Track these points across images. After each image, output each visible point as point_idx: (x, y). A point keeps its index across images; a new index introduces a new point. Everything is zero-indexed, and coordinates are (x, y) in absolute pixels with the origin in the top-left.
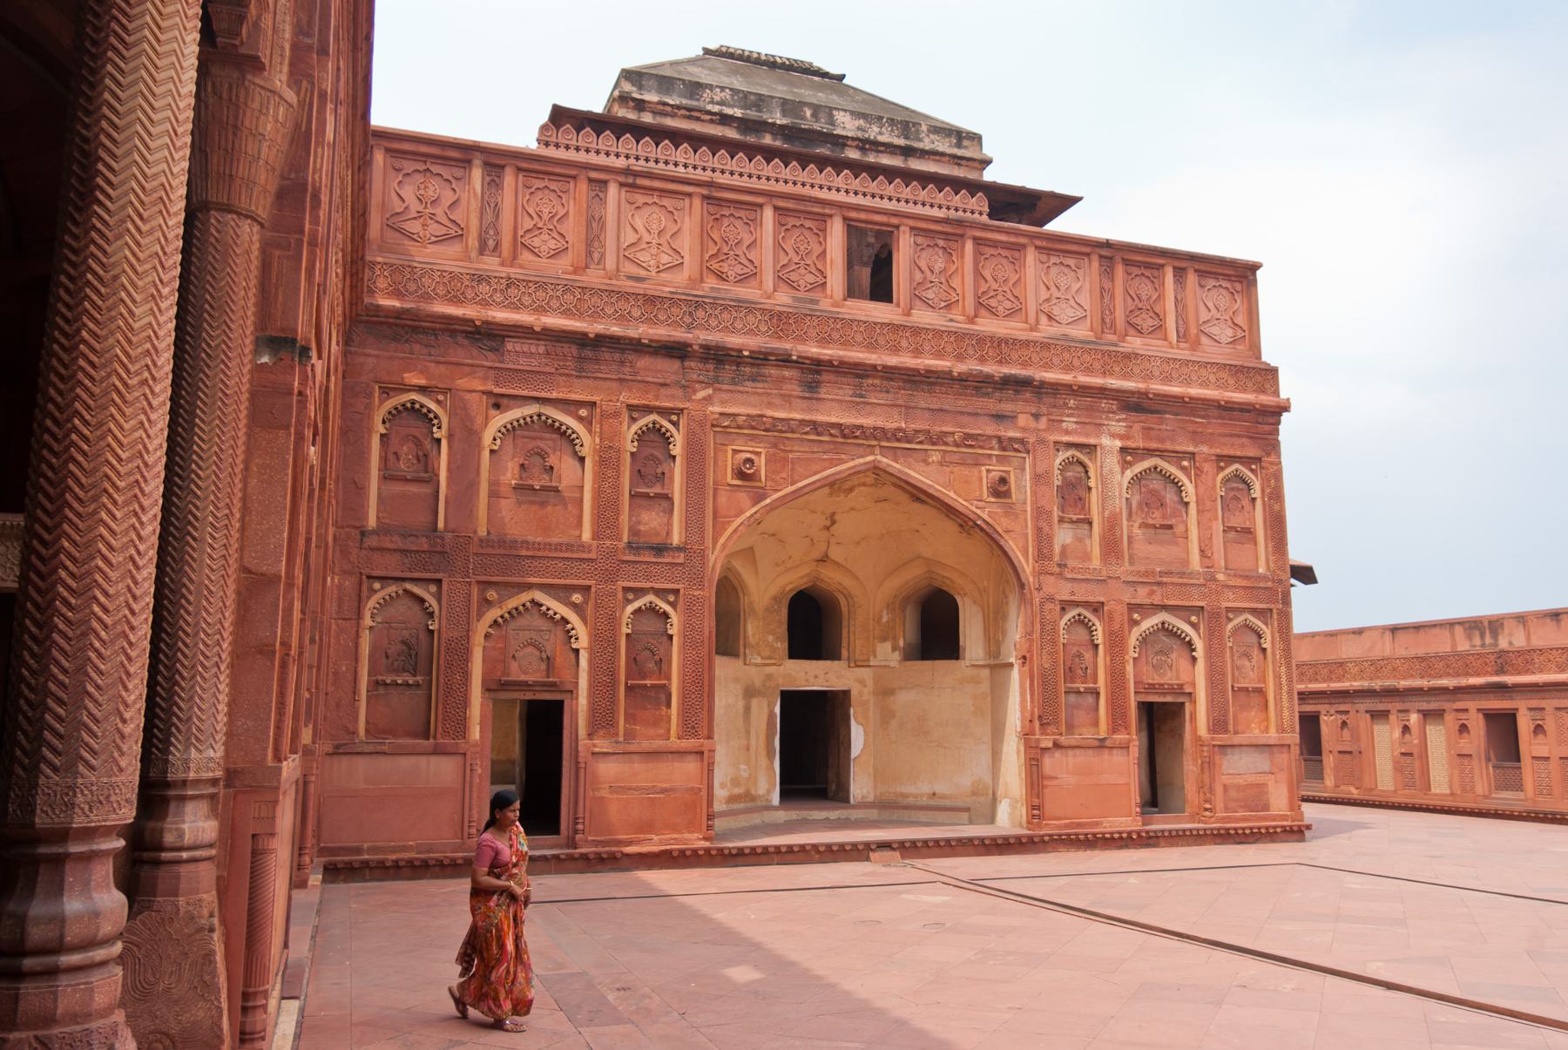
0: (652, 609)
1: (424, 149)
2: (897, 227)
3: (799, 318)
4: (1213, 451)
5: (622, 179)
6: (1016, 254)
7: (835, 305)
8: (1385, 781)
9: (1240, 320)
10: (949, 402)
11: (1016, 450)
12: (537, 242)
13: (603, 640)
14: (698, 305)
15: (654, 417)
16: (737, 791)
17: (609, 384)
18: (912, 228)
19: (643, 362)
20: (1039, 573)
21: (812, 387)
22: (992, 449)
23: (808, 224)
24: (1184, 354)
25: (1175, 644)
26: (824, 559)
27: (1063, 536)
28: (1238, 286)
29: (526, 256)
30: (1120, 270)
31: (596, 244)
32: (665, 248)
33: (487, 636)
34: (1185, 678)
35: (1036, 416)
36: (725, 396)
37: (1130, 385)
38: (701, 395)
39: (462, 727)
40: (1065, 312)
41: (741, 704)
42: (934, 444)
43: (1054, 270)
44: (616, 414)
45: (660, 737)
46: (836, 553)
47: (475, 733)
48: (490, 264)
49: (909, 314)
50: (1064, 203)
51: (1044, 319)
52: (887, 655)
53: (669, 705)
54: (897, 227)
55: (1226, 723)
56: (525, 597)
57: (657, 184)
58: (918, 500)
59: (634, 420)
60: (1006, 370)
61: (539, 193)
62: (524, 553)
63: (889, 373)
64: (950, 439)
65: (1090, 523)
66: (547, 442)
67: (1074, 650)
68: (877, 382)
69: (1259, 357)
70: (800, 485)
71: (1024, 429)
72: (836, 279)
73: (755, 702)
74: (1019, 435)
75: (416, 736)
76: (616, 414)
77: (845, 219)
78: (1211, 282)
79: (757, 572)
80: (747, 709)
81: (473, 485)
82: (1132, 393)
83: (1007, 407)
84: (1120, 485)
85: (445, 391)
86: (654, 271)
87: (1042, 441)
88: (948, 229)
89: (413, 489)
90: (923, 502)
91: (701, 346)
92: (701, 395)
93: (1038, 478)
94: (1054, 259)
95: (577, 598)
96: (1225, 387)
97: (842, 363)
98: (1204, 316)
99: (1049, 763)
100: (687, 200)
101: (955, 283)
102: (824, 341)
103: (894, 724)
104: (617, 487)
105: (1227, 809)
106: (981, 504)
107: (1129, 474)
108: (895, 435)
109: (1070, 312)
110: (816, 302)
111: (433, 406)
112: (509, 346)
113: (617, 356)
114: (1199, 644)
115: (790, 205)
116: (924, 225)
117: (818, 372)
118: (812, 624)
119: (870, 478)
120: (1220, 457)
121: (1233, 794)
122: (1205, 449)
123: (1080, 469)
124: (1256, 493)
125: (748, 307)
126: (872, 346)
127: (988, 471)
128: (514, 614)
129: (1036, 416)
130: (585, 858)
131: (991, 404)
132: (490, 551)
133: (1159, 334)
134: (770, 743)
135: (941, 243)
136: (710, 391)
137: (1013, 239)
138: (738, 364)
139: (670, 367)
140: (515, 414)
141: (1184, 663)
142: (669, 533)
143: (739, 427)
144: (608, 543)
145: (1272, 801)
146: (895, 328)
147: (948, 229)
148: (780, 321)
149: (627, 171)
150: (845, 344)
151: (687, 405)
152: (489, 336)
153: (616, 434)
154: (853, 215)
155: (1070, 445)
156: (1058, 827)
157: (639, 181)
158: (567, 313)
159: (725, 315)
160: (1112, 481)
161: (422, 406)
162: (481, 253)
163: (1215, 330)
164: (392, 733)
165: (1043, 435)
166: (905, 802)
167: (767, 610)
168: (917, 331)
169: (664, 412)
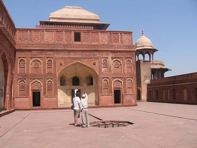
0: (50, 81)
7: (73, 43)
8: (185, 98)
10: (87, 53)
13: (44, 84)
16: (65, 102)
26: (76, 73)
27: (103, 69)
30: (112, 34)
33: (31, 85)
34: (120, 86)
36: (58, 55)
37: (112, 50)
39: (29, 95)
46: (77, 72)
47: (30, 95)
50: (108, 25)
52: (85, 85)
56: (35, 80)
60: (95, 49)
66: (38, 62)
72: (73, 39)
73: (68, 91)
75: (24, 96)
81: (29, 68)
83: (95, 54)
85: (25, 58)
87: (100, 58)
89: (23, 68)
93: (100, 62)
95: (41, 80)
98: (124, 39)
102: (70, 48)
107: (113, 61)
114: (122, 82)
120: (126, 58)
121: (127, 101)
128: (34, 82)
130: (43, 109)
131: (93, 53)
139: (51, 53)
140: (33, 59)
146: (79, 45)
149: (46, 29)
152: (30, 51)
153: (46, 61)
155: (104, 58)
157: (48, 30)
160: (111, 62)
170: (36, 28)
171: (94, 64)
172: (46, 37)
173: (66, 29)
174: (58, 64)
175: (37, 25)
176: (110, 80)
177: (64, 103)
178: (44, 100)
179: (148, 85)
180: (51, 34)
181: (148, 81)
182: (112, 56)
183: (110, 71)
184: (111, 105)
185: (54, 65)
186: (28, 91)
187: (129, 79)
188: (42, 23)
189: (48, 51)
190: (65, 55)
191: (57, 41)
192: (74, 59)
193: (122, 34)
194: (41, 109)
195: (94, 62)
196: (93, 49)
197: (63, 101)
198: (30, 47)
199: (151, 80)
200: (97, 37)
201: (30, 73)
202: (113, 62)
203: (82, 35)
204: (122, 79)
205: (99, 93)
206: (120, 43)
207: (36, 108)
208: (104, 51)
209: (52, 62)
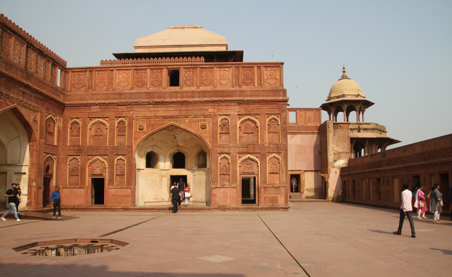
0: (121, 159)
1: (78, 70)
6: (211, 70)
7: (165, 89)
12: (100, 85)
13: (111, 165)
15: (122, 119)
20: (213, 146)
23: (158, 71)
24: (260, 88)
25: (253, 162)
26: (178, 146)
28: (277, 69)
30: (241, 69)
38: (131, 113)
41: (158, 179)
43: (222, 72)
44: (113, 119)
49: (182, 88)
51: (219, 84)
55: (266, 182)
57: (124, 68)
64: (191, 117)
66: (102, 126)
69: (283, 86)
75: (77, 185)
76: (113, 119)
77: (167, 68)
80: (161, 180)
87: (215, 115)
88: (193, 67)
89: (76, 137)
92: (131, 113)
94: (222, 69)
95: (106, 157)
98: (266, 77)
99: (214, 191)
108: (177, 117)
111: (79, 121)
114: (259, 162)
116: (186, 67)
118: (179, 161)
119: (174, 127)
121: (267, 199)
123: (226, 121)
124: (279, 123)
126: (171, 97)
128: (94, 161)
133: (252, 84)
135: (191, 70)
137: (210, 66)
141: (255, 167)
145: (279, 201)
146: (176, 92)
147: (193, 67)
148: (149, 94)
150: (164, 98)
153: (115, 124)
154: (169, 67)
163: (269, 81)
164: (73, 184)
168: (182, 92)
170: (101, 66)
171: (203, 127)
172: (118, 80)
173: (152, 64)
174: (135, 129)
175: (102, 61)
178: (110, 191)
179: (342, 170)
180: (126, 75)
181: (342, 162)
182: (238, 112)
184: (234, 205)
188: (119, 56)
193: (262, 68)
194: (104, 209)
195: (203, 123)
198: (88, 100)
199: (350, 161)
200: (210, 75)
201: (88, 145)
202: (242, 123)
203: (183, 75)
204: (258, 156)
206: (256, 85)
209: (126, 125)
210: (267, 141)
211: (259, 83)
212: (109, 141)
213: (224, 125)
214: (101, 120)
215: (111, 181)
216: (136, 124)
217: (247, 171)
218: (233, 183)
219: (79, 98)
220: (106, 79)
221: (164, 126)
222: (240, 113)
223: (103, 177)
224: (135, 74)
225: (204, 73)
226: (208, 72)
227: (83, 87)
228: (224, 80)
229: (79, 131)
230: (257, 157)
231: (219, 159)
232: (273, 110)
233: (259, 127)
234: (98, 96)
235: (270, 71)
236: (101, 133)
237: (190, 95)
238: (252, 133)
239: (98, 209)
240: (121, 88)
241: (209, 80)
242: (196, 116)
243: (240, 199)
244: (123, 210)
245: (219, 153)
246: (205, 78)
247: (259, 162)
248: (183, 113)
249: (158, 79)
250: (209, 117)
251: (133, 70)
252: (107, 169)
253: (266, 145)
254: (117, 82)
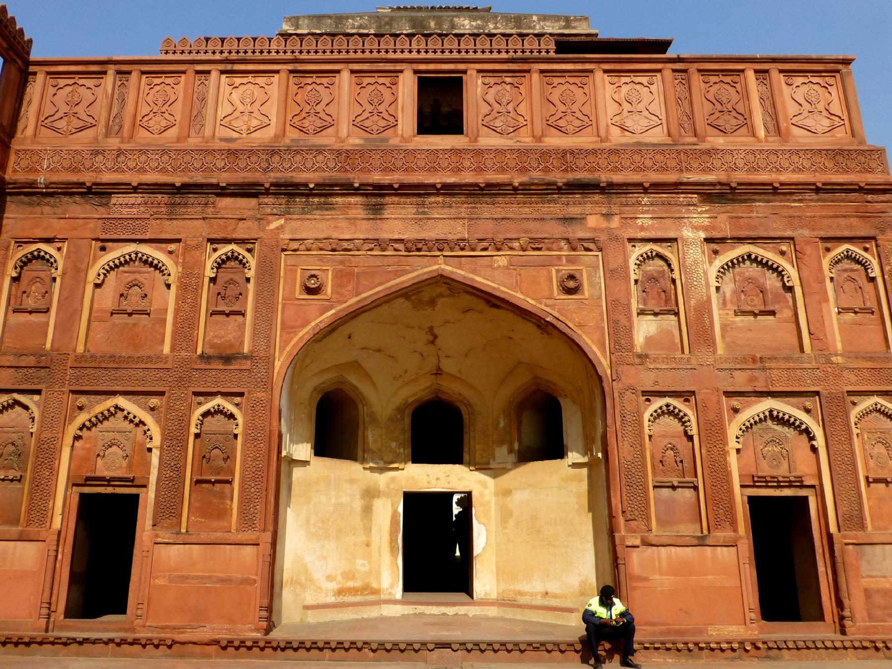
2: (465, 72)
3: (361, 152)
4: (816, 233)
5: (222, 67)
9: (836, 108)
11: (587, 249)
13: (174, 439)
14: (273, 152)
17: (195, 222)
18: (479, 71)
19: (225, 202)
21: (376, 210)
22: (561, 249)
29: (143, 133)
30: (697, 80)
31: (199, 118)
32: (256, 114)
35: (608, 216)
36: (295, 224)
38: (274, 225)
40: (636, 123)
42: (499, 250)
44: (198, 247)
45: (221, 529)
48: (114, 143)
49: (476, 141)
51: (615, 131)
53: (232, 500)
54: (465, 72)
55: (862, 518)
58: (495, 306)
59: (215, 250)
60: (571, 176)
61: (158, 88)
62: (111, 365)
63: (449, 190)
64: (516, 245)
65: (677, 314)
67: (665, 442)
68: (440, 199)
70: (363, 295)
71: (595, 230)
74: (588, 235)
76: (198, 247)
78: (799, 80)
79: (374, 385)
82: (713, 184)
83: (574, 211)
84: (705, 273)
86: (244, 135)
87: (617, 239)
90: (498, 307)
91: (272, 185)
92: (274, 225)
93: (615, 274)
96: (825, 169)
97: (403, 186)
100: (277, 76)
101: (522, 109)
102: (386, 170)
103: (511, 523)
104: (196, 307)
105: (871, 617)
106: (549, 302)
107: (720, 261)
108: (461, 244)
109: (645, 123)
110: (387, 140)
112: (113, 201)
113: (202, 199)
114: (817, 431)
115: (366, 67)
117: (383, 195)
119: (443, 289)
120: (824, 239)
121: (878, 600)
122: (806, 232)
124: (876, 272)
125: (320, 150)
126: (433, 170)
127: (558, 271)
129: (608, 216)
132: (83, 365)
133: (744, 130)
134: (393, 541)
136: (282, 221)
138: (307, 195)
142: (242, 343)
143: (308, 250)
144: (183, 353)
146: (454, 151)
151: (261, 234)
156: (654, 634)
158: (164, 171)
159: (298, 158)
161: (46, 253)
162: (107, 135)
163: (809, 122)
165: (617, 232)
166: (522, 600)
167: (391, 419)
168: (479, 152)
169: (241, 242)
170: (163, 57)
171: (571, 284)
174: (289, 287)
175: (168, 41)
176: (712, 416)
177: (340, 592)
178: (160, 558)
180: (257, 91)
182: (705, 229)
183: (701, 333)
185: (257, 294)
186: (42, 489)
187: (868, 402)
189: (222, 191)
190: (347, 221)
191: (292, 134)
192: (416, 247)
195: (567, 269)
196: (560, 178)
197: (330, 578)
201: (80, 349)
205: (621, 520)
206: (761, 133)
207: (80, 635)
208: (646, 191)
209: (251, 274)
210: (839, 346)
211: (771, 127)
212: (174, 334)
213: (653, 279)
214: (145, 249)
215: (168, 510)
216: (291, 269)
217: (766, 470)
218: (718, 526)
219: (66, 164)
220: (179, 105)
221: (405, 279)
222: (716, 234)
223: (134, 491)
224: (293, 88)
225: (557, 92)
226: (573, 87)
227: (81, 129)
228: (636, 117)
229: (47, 293)
230: (808, 411)
231: (647, 416)
232: (843, 222)
233: (798, 290)
234: (143, 158)
235: (805, 88)
236: (142, 305)
237: (512, 164)
238: (773, 313)
239: (95, 642)
240: (237, 135)
241: (578, 114)
242: (536, 244)
243: (752, 598)
244: (213, 648)
245: (644, 393)
246: (563, 108)
247: (817, 431)
248: (486, 229)
249: (381, 108)
250: (591, 246)
251: (283, 75)
252: (156, 453)
253: (840, 360)
254: (221, 113)
